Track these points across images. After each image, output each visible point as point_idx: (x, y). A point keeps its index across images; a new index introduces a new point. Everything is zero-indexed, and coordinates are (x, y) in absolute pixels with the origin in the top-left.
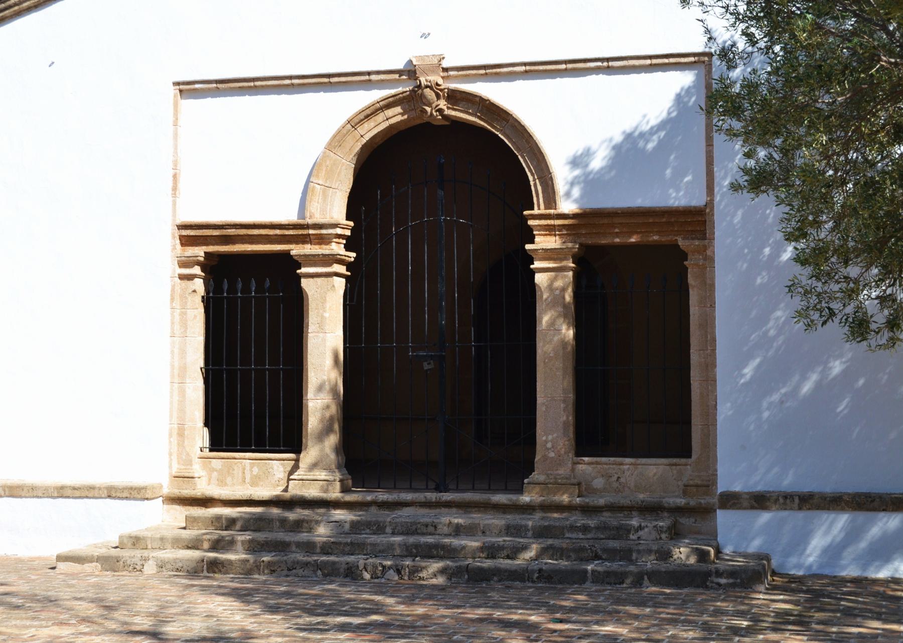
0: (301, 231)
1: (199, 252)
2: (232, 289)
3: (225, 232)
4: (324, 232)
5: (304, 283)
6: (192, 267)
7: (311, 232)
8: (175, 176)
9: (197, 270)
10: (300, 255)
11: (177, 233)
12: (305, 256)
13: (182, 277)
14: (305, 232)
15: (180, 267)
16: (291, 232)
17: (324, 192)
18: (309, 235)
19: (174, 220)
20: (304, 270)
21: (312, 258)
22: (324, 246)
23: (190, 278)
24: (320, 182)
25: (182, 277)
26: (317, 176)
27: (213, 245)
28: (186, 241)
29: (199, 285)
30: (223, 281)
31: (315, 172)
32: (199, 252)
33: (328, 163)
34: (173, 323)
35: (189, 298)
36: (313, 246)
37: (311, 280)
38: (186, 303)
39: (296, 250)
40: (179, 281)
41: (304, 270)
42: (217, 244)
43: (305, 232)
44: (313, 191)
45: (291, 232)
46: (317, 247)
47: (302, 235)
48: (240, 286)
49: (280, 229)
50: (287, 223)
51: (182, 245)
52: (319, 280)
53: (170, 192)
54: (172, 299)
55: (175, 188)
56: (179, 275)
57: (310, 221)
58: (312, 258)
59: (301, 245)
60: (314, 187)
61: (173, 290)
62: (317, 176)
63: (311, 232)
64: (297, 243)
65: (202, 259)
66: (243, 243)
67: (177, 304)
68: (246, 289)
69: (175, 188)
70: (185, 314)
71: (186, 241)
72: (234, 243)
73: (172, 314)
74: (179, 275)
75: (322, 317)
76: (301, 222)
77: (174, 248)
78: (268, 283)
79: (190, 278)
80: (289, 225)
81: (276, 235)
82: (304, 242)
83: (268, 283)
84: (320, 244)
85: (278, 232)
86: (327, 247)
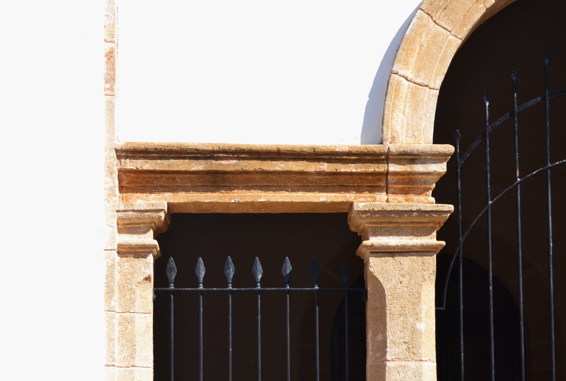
0: (370, 166)
1: (158, 202)
2: (216, 276)
3: (216, 166)
4: (419, 168)
5: (375, 265)
6: (145, 232)
7: (393, 168)
8: (110, 56)
9: (148, 239)
10: (373, 212)
11: (116, 165)
12: (384, 213)
13: (125, 251)
14: (381, 168)
15: (120, 231)
16: (352, 168)
17: (414, 95)
18: (387, 173)
19: (110, 140)
20: (374, 241)
21: (397, 218)
22: (416, 198)
23: (137, 252)
24: (410, 76)
25: (125, 251)
26: (406, 64)
27: (187, 190)
28: (131, 182)
29: (147, 266)
30: (196, 261)
31: (401, 54)
32: (158, 202)
33: (424, 38)
34: (111, 340)
35: (138, 292)
36: (391, 197)
37: (390, 259)
38: (132, 301)
39: (362, 202)
40: (118, 258)
41: (374, 241)
42: (195, 189)
43: (381, 168)
44: (397, 90)
45: (352, 168)
46: (400, 197)
47: (373, 174)
48: (231, 272)
49: (329, 161)
50: (346, 149)
51: (122, 189)
52: (406, 261)
53: (102, 84)
54: (109, 293)
55: (111, 79)
56: (120, 246)
57: (394, 148)
58: (397, 218)
59: (366, 194)
60: (399, 83)
61: (110, 276)
62: (406, 64)
63: (393, 168)
64: (359, 189)
65: (162, 215)
66: (248, 188)
67: (115, 303)
68: (244, 276)
69: (111, 79)
70: (131, 321)
71: (131, 182)
72: (229, 188)
73: (109, 322)
74: (120, 246)
75: (414, 331)
76: (375, 147)
77: (111, 195)
78: (288, 268)
79: (137, 252)
80: (350, 154)
81: (319, 173)
82: (373, 189)
83: (288, 268)
84: (405, 192)
85: (325, 167)
86: (422, 198)
